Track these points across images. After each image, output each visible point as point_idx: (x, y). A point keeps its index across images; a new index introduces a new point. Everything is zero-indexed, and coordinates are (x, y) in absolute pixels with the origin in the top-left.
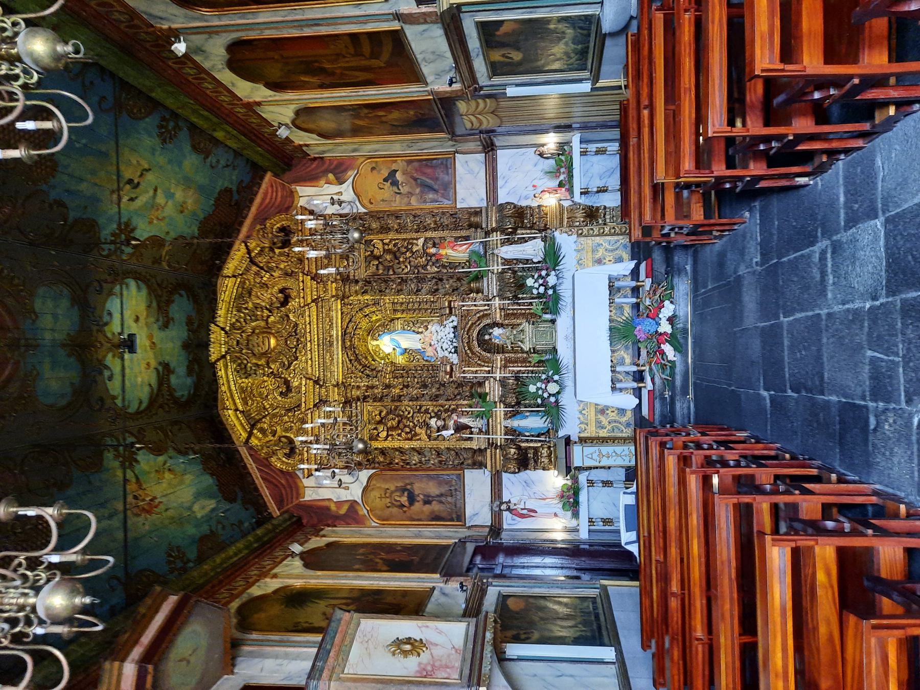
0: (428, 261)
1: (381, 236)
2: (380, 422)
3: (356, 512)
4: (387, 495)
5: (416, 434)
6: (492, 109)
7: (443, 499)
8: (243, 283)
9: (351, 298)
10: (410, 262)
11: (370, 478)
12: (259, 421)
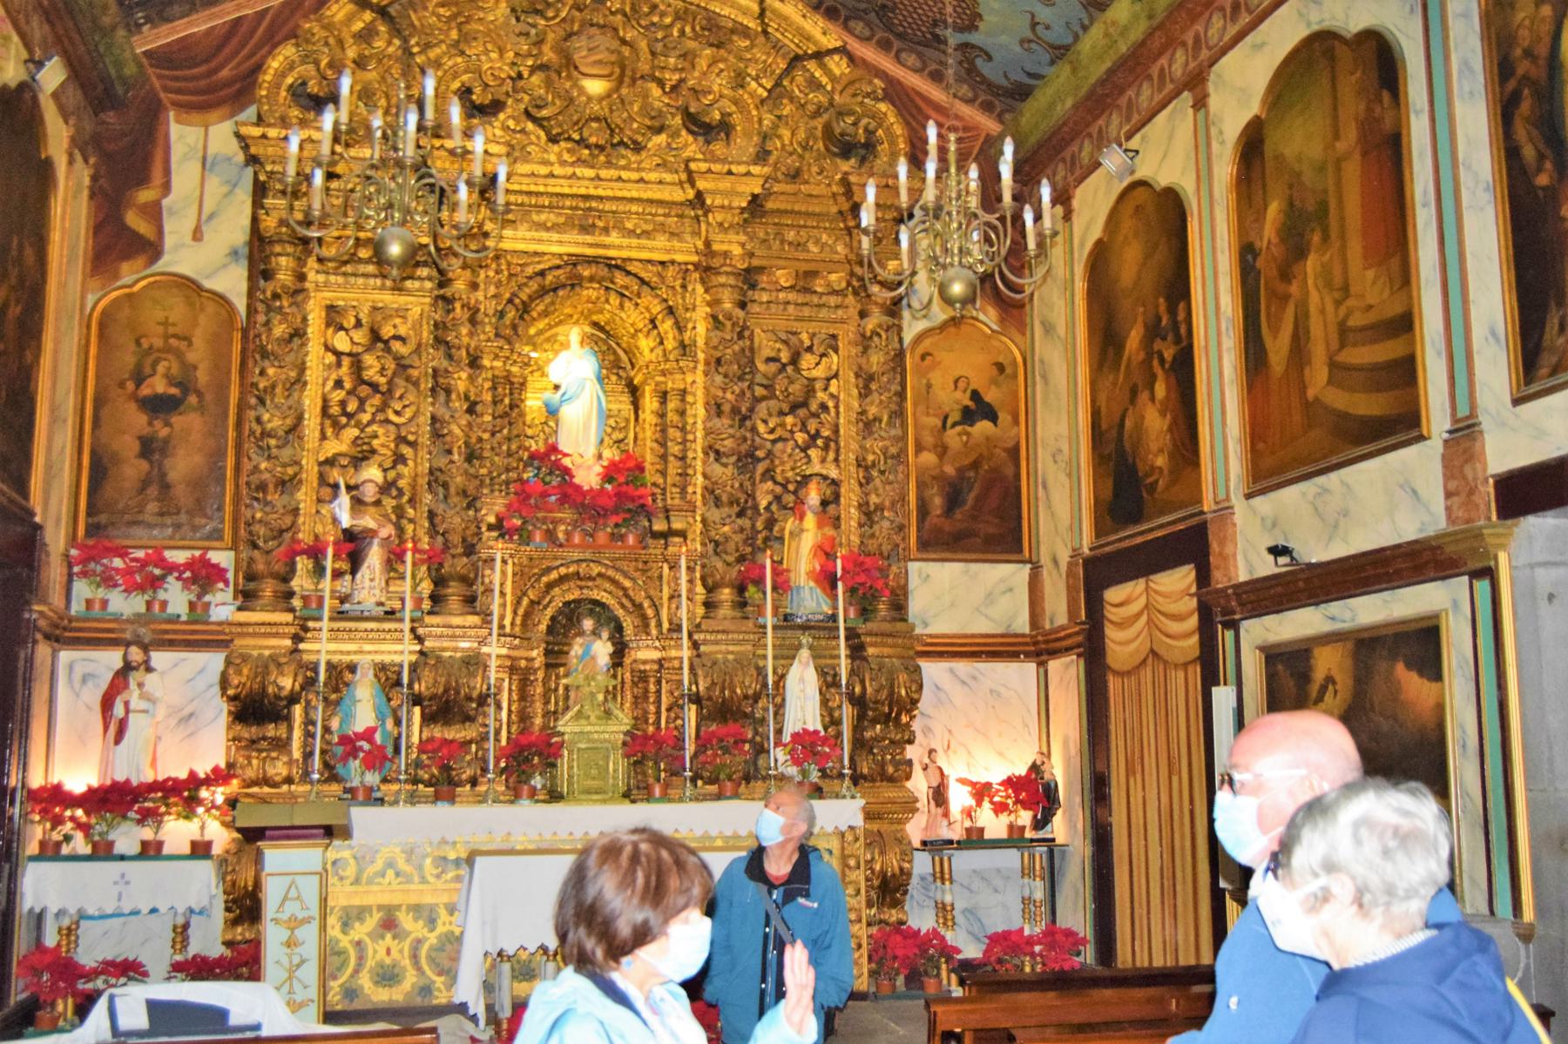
0: (784, 486)
2: (375, 336)
3: (127, 256)
4: (172, 341)
6: (1162, 652)
7: (153, 491)
8: (745, 32)
9: (700, 289)
11: (221, 299)
12: (396, 31)
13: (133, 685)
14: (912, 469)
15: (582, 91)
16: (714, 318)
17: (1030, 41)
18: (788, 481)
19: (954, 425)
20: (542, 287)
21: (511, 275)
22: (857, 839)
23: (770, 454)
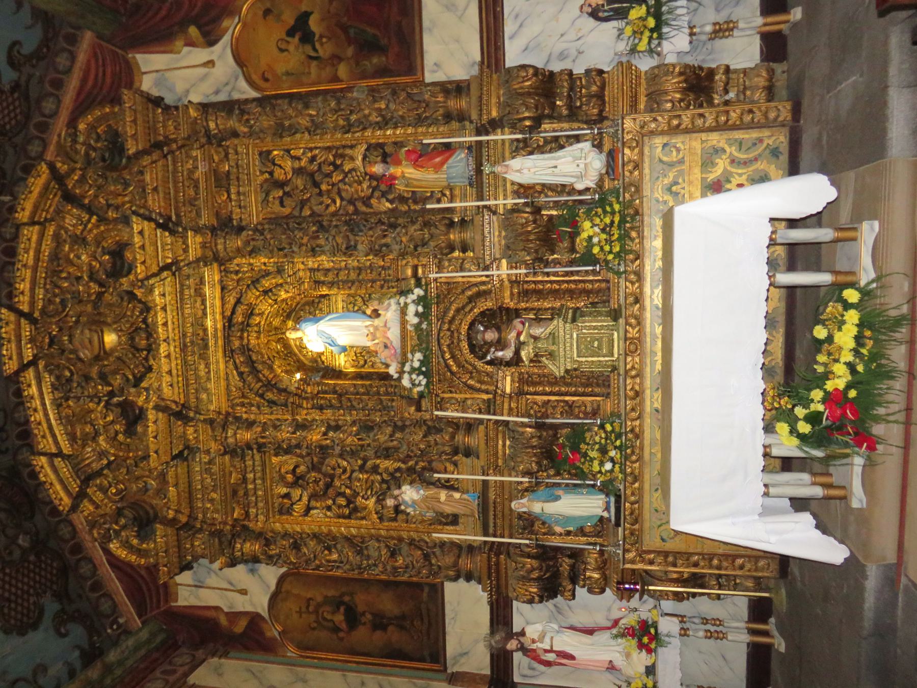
0: (375, 189)
2: (294, 484)
3: (262, 633)
4: (311, 609)
5: (356, 510)
9: (236, 261)
11: (281, 580)
12: (99, 473)
13: (534, 646)
15: (113, 350)
16: (251, 253)
20: (251, 373)
21: (243, 396)
22: (655, 120)
23: (351, 202)
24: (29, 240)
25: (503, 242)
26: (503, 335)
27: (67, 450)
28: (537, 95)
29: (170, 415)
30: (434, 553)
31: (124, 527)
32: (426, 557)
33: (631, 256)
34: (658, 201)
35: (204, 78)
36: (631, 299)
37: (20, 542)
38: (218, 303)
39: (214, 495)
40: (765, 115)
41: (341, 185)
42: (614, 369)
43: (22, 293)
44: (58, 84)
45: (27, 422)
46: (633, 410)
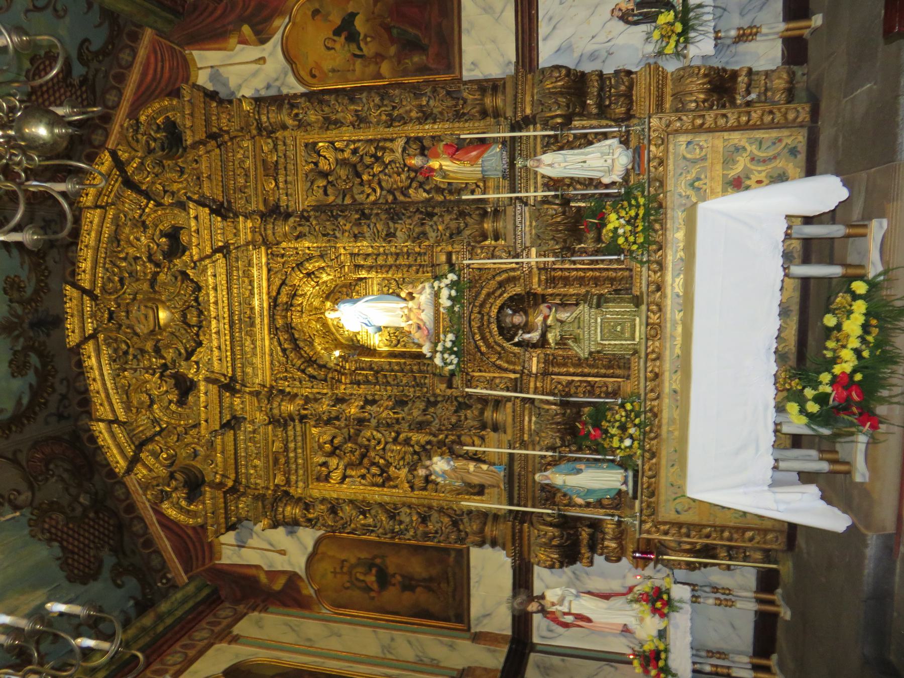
0: (412, 180)
1: (332, 134)
2: (332, 454)
3: (299, 591)
4: (345, 570)
5: (389, 479)
8: (116, 218)
10: (379, 184)
11: (318, 543)
12: (150, 440)
13: (553, 609)
14: (393, 81)
15: (167, 325)
16: (297, 238)
17: (55, 10)
18: (408, 177)
19: (360, 49)
21: (286, 371)
22: (680, 119)
23: (390, 191)
24: (91, 222)
25: (534, 232)
26: (531, 318)
27: (122, 417)
28: (568, 93)
29: (219, 387)
30: (462, 520)
31: (176, 489)
32: (455, 524)
33: (654, 247)
34: (680, 195)
35: (255, 74)
36: (652, 288)
37: (81, 500)
38: (265, 284)
39: (257, 462)
40: (785, 115)
41: (382, 176)
42: (636, 352)
43: (84, 271)
44: (121, 78)
45: (87, 391)
46: (652, 391)
